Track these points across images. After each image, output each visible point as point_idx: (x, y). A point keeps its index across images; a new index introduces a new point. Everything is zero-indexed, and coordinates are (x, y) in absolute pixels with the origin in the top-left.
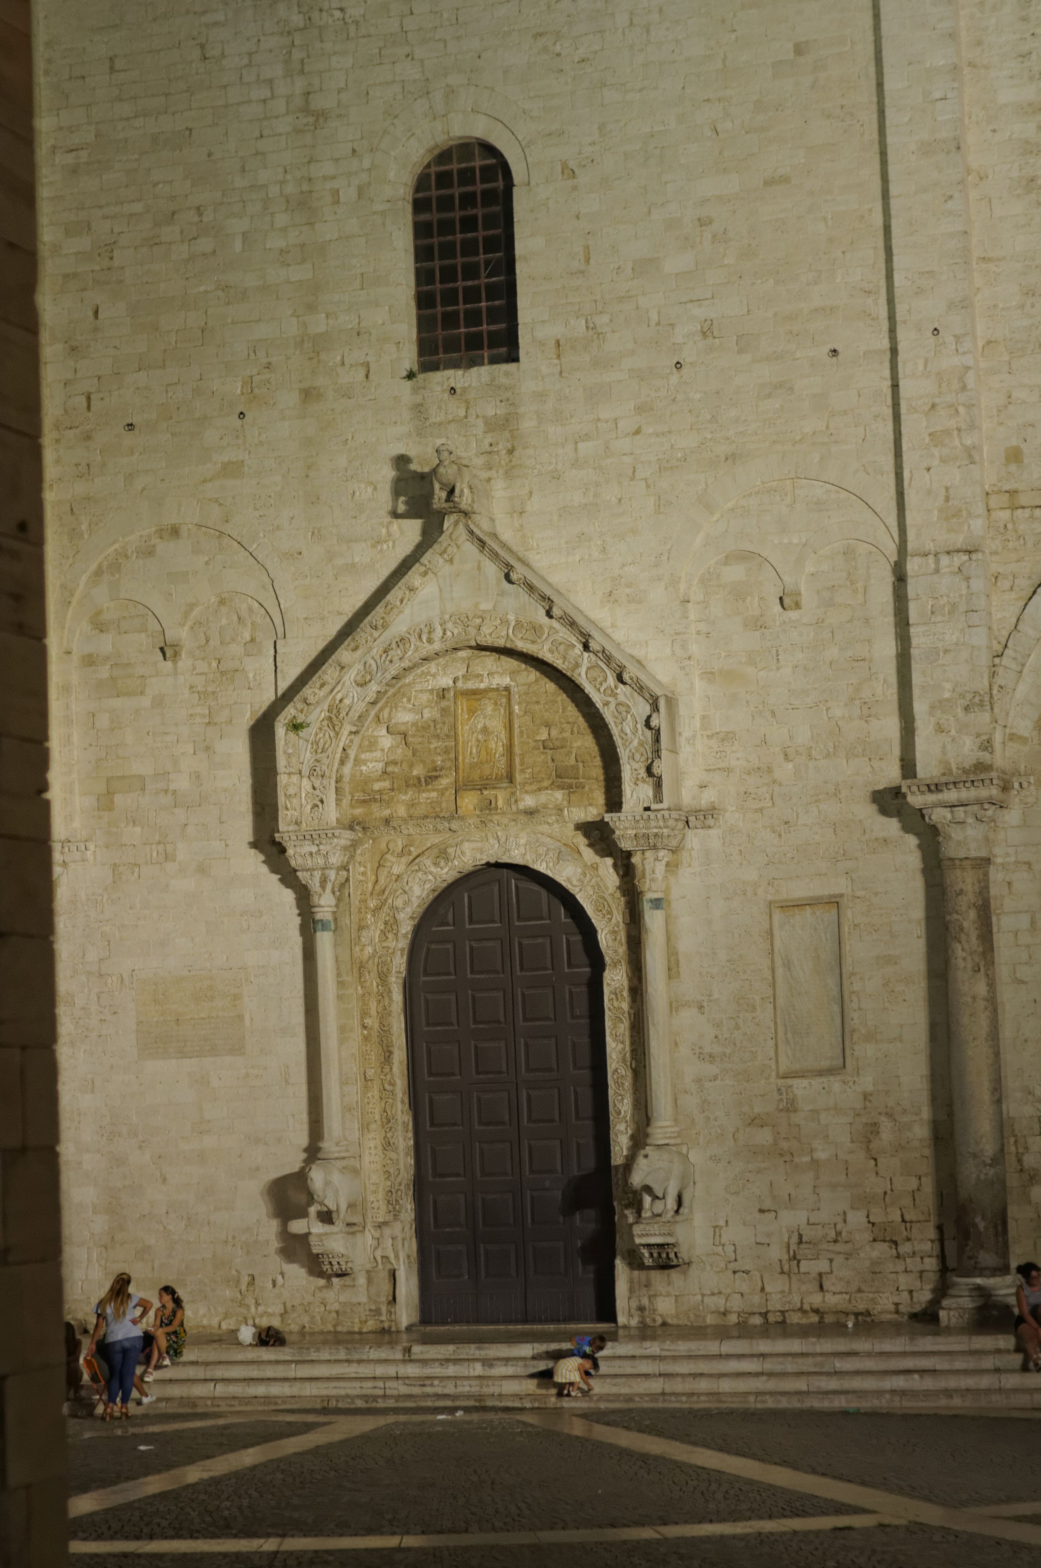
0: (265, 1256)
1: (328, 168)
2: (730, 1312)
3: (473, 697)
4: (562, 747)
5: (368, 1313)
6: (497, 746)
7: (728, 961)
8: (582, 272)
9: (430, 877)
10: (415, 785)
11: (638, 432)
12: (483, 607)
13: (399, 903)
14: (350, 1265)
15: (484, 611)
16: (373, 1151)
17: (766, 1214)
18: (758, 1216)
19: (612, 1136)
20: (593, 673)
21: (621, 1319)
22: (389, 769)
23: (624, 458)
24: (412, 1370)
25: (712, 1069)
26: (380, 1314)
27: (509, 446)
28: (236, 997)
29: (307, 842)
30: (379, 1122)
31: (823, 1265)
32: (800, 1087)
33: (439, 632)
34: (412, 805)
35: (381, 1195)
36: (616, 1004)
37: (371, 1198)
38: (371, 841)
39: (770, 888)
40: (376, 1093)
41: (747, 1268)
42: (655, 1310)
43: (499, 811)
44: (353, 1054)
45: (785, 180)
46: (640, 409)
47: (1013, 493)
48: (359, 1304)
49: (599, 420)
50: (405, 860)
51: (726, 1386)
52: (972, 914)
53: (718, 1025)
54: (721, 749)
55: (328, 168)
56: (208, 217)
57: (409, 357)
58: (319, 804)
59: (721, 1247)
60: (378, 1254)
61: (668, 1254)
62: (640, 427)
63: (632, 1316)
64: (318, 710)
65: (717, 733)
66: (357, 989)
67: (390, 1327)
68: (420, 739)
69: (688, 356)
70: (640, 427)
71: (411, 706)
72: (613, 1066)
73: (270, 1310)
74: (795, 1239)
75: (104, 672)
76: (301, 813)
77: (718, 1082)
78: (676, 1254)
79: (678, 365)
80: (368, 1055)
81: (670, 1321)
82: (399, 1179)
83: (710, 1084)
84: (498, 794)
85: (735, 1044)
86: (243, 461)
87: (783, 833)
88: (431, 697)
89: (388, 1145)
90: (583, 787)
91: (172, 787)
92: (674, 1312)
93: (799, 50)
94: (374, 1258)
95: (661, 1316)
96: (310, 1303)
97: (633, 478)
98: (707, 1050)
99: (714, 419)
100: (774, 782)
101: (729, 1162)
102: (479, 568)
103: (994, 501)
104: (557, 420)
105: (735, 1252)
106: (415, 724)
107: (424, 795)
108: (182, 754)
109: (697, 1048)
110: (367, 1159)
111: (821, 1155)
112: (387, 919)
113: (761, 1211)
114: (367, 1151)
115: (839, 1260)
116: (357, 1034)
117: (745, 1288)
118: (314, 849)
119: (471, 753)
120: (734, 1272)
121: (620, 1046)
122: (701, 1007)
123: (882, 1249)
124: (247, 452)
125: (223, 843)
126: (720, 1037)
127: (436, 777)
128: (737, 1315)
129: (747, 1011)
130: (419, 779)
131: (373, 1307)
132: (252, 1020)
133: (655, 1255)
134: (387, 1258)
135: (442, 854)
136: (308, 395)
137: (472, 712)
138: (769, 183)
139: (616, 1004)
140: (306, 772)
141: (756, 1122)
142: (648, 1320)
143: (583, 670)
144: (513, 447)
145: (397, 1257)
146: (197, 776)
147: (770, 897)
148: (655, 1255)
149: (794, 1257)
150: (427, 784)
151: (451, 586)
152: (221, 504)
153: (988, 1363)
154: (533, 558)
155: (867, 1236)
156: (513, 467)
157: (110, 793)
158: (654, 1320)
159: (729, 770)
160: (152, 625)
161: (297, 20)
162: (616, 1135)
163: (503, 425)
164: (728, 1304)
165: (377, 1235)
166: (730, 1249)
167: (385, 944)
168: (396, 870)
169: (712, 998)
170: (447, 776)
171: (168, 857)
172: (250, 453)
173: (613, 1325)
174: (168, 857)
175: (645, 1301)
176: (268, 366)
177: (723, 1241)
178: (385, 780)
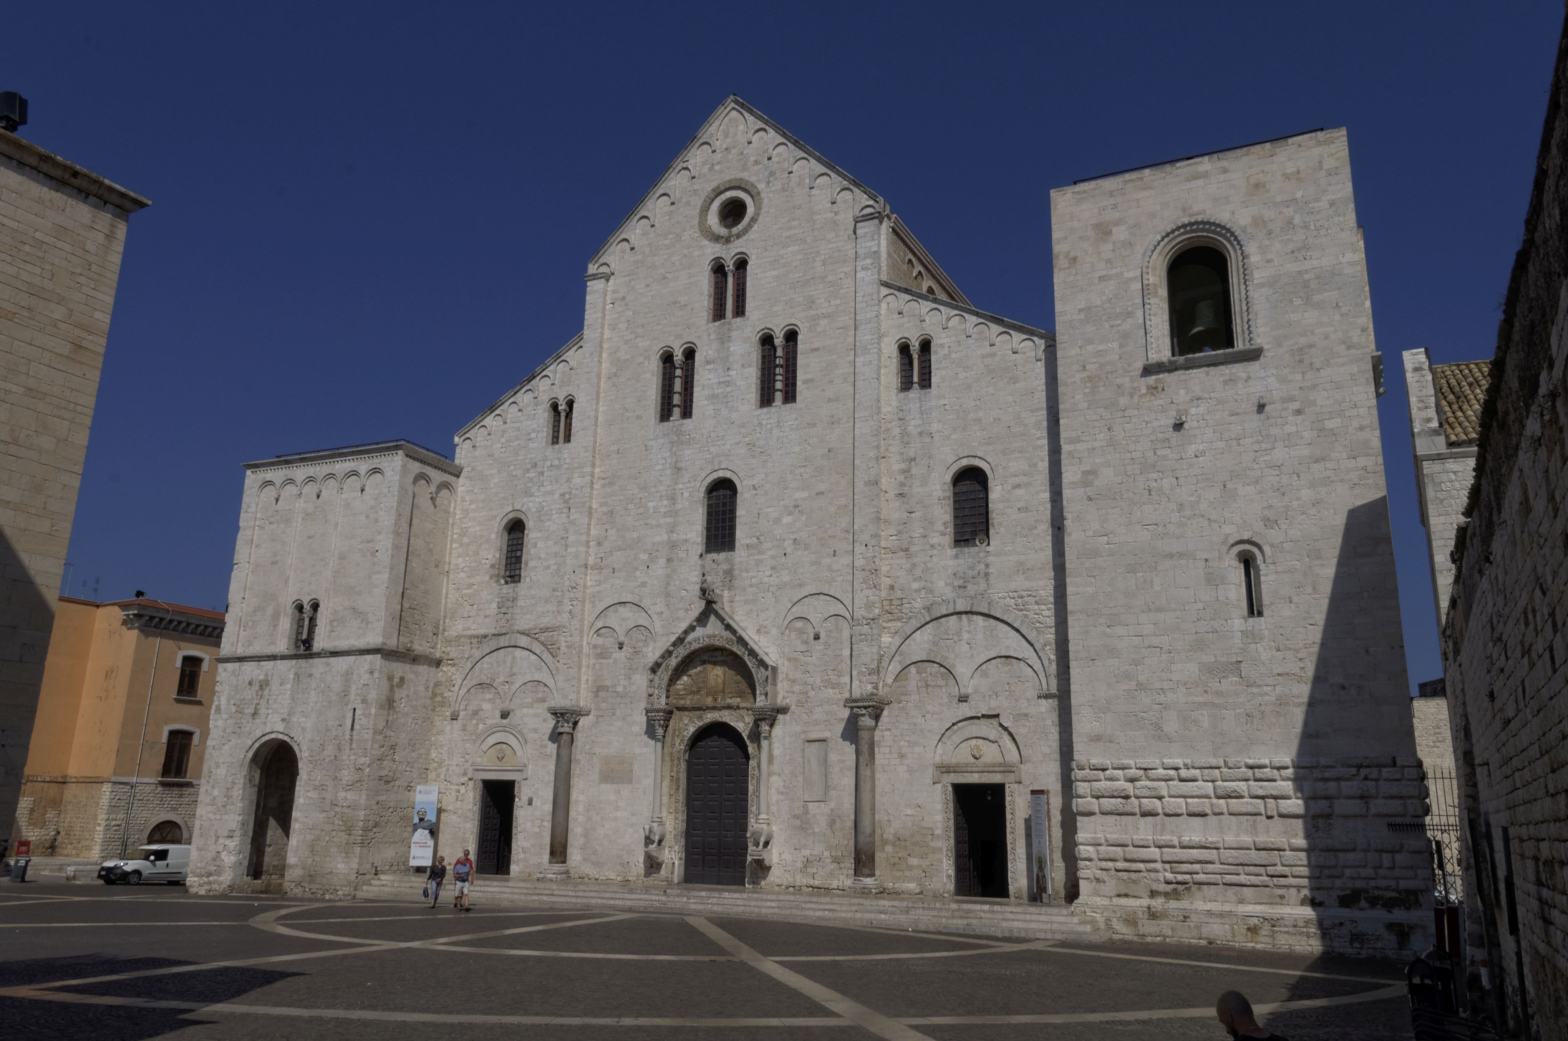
1: (681, 486)
6: (720, 680)
8: (757, 522)
11: (771, 576)
13: (685, 734)
24: (664, 898)
25: (782, 797)
28: (631, 764)
31: (814, 870)
32: (810, 805)
33: (701, 641)
34: (692, 699)
45: (822, 493)
47: (891, 600)
51: (764, 911)
52: (867, 746)
53: (785, 782)
55: (681, 486)
56: (643, 501)
57: (700, 548)
69: (789, 551)
74: (805, 859)
75: (599, 651)
89: (676, 818)
93: (829, 451)
103: (885, 603)
111: (816, 830)
115: (820, 868)
122: (779, 775)
123: (834, 866)
135: (700, 718)
136: (669, 560)
137: (713, 669)
138: (817, 494)
141: (796, 817)
146: (625, 687)
149: (805, 866)
153: (854, 908)
154: (736, 617)
155: (830, 860)
157: (598, 691)
159: (793, 693)
160: (615, 635)
161: (675, 438)
168: (686, 722)
174: (614, 714)
176: (657, 551)
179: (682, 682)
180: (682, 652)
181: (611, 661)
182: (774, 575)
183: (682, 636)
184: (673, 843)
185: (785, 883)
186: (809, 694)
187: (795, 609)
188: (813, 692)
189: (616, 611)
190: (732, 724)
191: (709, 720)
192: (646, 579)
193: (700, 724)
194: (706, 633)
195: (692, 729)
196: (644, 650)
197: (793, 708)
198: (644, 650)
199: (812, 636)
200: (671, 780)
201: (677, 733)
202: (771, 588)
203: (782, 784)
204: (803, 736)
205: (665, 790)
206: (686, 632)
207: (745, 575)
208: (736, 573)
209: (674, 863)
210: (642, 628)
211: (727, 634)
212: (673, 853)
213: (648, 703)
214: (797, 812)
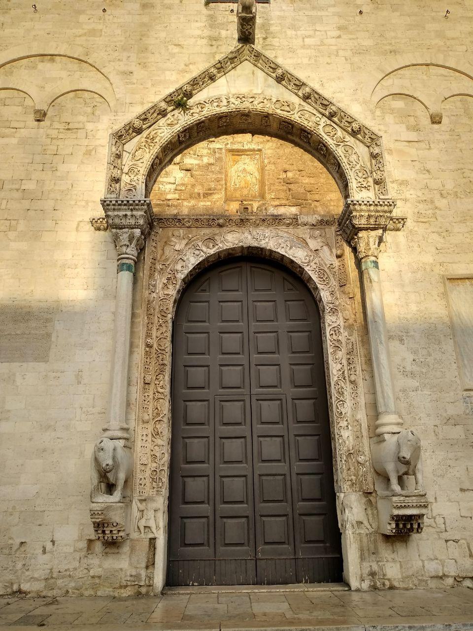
0: (40, 525)
2: (448, 576)
3: (236, 153)
4: (296, 183)
5: (129, 578)
7: (418, 311)
9: (202, 253)
10: (196, 198)
11: (339, 37)
12: (255, 92)
13: (179, 267)
14: (121, 534)
15: (256, 94)
16: (144, 438)
17: (467, 493)
18: (461, 495)
19: (336, 431)
20: (328, 129)
21: (354, 583)
22: (179, 188)
23: (332, 47)
26: (140, 580)
27: (264, 36)
28: (48, 320)
29: (122, 207)
30: (151, 416)
33: (225, 102)
35: (148, 473)
36: (334, 337)
37: (139, 475)
38: (161, 230)
39: (441, 267)
40: (151, 393)
41: (457, 537)
42: (384, 575)
43: (254, 214)
44: (136, 364)
46: (339, 28)
48: (121, 569)
49: (316, 30)
50: (184, 242)
53: (415, 352)
54: (400, 188)
58: (134, 190)
59: (433, 520)
60: (142, 523)
61: (412, 525)
62: (340, 35)
63: (363, 580)
64: (139, 136)
65: (396, 180)
66: (144, 318)
67: (147, 592)
68: (201, 173)
70: (340, 35)
71: (196, 156)
72: (336, 379)
73: (36, 575)
76: (119, 193)
77: (419, 392)
78: (419, 524)
79: (361, 12)
80: (148, 365)
81: (396, 584)
82: (162, 462)
83: (413, 393)
84: (254, 204)
85: (429, 366)
86: (101, 30)
87: (446, 237)
88: (209, 151)
89: (156, 434)
90: (311, 205)
91: (23, 187)
92: (400, 576)
94: (138, 527)
95: (389, 580)
96: (75, 569)
97: (337, 55)
98: (409, 368)
99: (381, 36)
100: (436, 208)
101: (433, 452)
102: (253, 73)
104: (292, 28)
105: (444, 523)
106: (198, 165)
107: (202, 203)
108: (34, 170)
109: (401, 368)
110: (139, 444)
112: (169, 276)
113: (462, 490)
114: (140, 437)
116: (141, 350)
117: (456, 555)
118: (129, 213)
119: (235, 182)
120: (447, 541)
121: (339, 366)
122: (401, 340)
124: (105, 26)
125: (54, 222)
126: (417, 360)
127: (211, 194)
128: (453, 579)
129: (435, 344)
130: (199, 194)
131: (134, 573)
132: (58, 336)
133: (401, 526)
134: (149, 527)
135: (211, 239)
137: (236, 162)
139: (334, 337)
140: (126, 169)
142: (378, 584)
143: (321, 127)
144: (266, 37)
145: (157, 527)
147: (442, 273)
148: (401, 526)
150: (204, 197)
151: (235, 81)
152: (84, 47)
156: (267, 45)
158: (384, 584)
162: (339, 430)
163: (261, 27)
164: (445, 569)
165: (142, 507)
166: (440, 521)
167: (166, 292)
168: (177, 247)
169: (408, 334)
170: (218, 193)
171: (10, 228)
172: (106, 27)
173: (347, 589)
175: (375, 567)
177: (434, 515)
178: (175, 193)
179: (172, 180)
180: (182, 120)
181: (14, 141)
182: (344, 37)
183: (189, 88)
184: (148, 492)
185: (452, 571)
186: (437, 204)
187: (387, 82)
188: (445, 201)
189: (35, 68)
190: (282, 252)
191: (229, 245)
192: (100, 27)
193: (212, 252)
194: (233, 91)
195: (192, 261)
196: (90, 126)
197: (409, 223)
198: (90, 126)
199: (426, 121)
200: (147, 354)
201: (159, 267)
202: (341, 53)
203: (411, 357)
204: (439, 270)
205: (137, 375)
206: (196, 83)
207: (290, 33)
208: (273, 29)
209: (152, 541)
210: (86, 94)
211: (277, 92)
212: (151, 514)
213: (110, 191)
214: (452, 411)
